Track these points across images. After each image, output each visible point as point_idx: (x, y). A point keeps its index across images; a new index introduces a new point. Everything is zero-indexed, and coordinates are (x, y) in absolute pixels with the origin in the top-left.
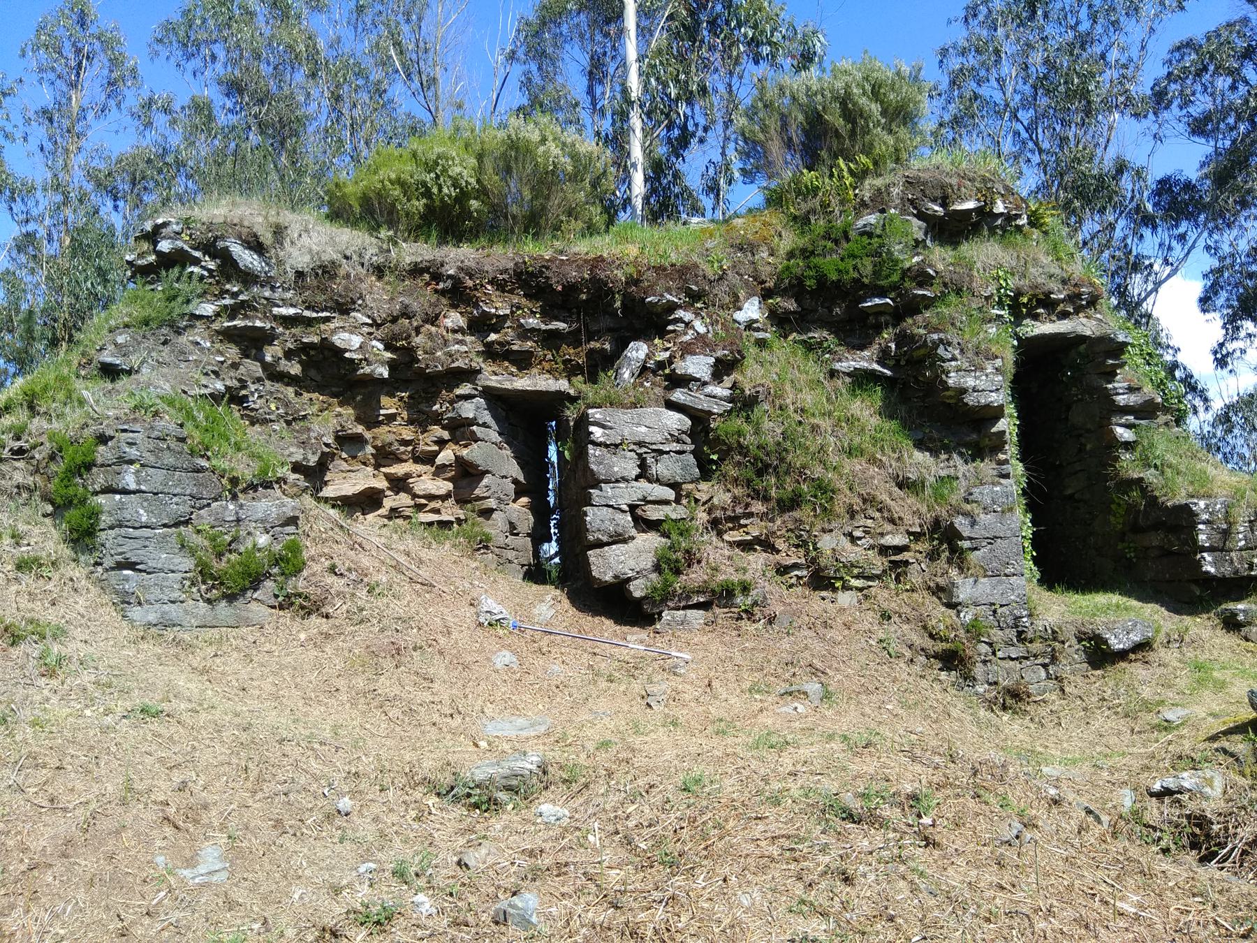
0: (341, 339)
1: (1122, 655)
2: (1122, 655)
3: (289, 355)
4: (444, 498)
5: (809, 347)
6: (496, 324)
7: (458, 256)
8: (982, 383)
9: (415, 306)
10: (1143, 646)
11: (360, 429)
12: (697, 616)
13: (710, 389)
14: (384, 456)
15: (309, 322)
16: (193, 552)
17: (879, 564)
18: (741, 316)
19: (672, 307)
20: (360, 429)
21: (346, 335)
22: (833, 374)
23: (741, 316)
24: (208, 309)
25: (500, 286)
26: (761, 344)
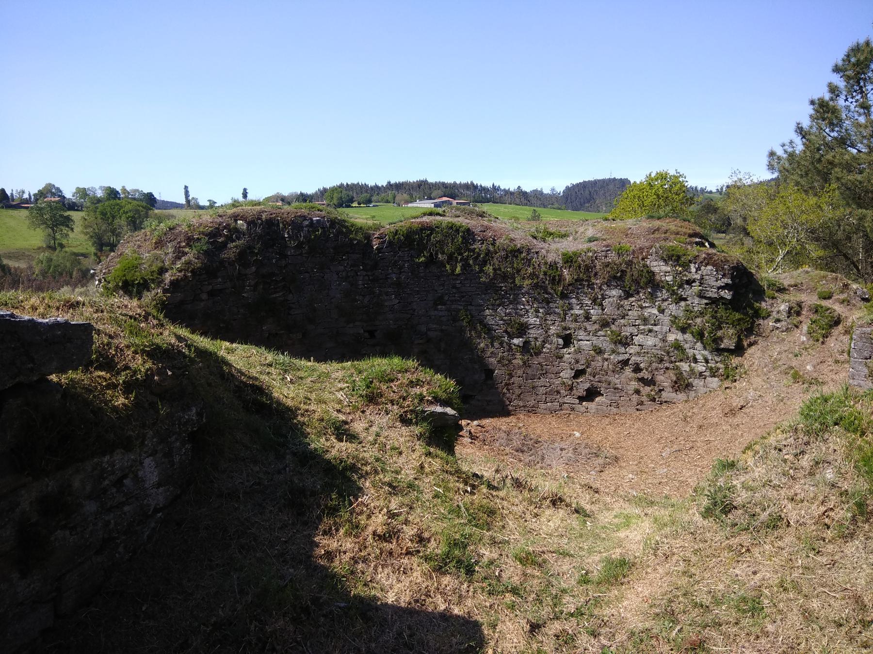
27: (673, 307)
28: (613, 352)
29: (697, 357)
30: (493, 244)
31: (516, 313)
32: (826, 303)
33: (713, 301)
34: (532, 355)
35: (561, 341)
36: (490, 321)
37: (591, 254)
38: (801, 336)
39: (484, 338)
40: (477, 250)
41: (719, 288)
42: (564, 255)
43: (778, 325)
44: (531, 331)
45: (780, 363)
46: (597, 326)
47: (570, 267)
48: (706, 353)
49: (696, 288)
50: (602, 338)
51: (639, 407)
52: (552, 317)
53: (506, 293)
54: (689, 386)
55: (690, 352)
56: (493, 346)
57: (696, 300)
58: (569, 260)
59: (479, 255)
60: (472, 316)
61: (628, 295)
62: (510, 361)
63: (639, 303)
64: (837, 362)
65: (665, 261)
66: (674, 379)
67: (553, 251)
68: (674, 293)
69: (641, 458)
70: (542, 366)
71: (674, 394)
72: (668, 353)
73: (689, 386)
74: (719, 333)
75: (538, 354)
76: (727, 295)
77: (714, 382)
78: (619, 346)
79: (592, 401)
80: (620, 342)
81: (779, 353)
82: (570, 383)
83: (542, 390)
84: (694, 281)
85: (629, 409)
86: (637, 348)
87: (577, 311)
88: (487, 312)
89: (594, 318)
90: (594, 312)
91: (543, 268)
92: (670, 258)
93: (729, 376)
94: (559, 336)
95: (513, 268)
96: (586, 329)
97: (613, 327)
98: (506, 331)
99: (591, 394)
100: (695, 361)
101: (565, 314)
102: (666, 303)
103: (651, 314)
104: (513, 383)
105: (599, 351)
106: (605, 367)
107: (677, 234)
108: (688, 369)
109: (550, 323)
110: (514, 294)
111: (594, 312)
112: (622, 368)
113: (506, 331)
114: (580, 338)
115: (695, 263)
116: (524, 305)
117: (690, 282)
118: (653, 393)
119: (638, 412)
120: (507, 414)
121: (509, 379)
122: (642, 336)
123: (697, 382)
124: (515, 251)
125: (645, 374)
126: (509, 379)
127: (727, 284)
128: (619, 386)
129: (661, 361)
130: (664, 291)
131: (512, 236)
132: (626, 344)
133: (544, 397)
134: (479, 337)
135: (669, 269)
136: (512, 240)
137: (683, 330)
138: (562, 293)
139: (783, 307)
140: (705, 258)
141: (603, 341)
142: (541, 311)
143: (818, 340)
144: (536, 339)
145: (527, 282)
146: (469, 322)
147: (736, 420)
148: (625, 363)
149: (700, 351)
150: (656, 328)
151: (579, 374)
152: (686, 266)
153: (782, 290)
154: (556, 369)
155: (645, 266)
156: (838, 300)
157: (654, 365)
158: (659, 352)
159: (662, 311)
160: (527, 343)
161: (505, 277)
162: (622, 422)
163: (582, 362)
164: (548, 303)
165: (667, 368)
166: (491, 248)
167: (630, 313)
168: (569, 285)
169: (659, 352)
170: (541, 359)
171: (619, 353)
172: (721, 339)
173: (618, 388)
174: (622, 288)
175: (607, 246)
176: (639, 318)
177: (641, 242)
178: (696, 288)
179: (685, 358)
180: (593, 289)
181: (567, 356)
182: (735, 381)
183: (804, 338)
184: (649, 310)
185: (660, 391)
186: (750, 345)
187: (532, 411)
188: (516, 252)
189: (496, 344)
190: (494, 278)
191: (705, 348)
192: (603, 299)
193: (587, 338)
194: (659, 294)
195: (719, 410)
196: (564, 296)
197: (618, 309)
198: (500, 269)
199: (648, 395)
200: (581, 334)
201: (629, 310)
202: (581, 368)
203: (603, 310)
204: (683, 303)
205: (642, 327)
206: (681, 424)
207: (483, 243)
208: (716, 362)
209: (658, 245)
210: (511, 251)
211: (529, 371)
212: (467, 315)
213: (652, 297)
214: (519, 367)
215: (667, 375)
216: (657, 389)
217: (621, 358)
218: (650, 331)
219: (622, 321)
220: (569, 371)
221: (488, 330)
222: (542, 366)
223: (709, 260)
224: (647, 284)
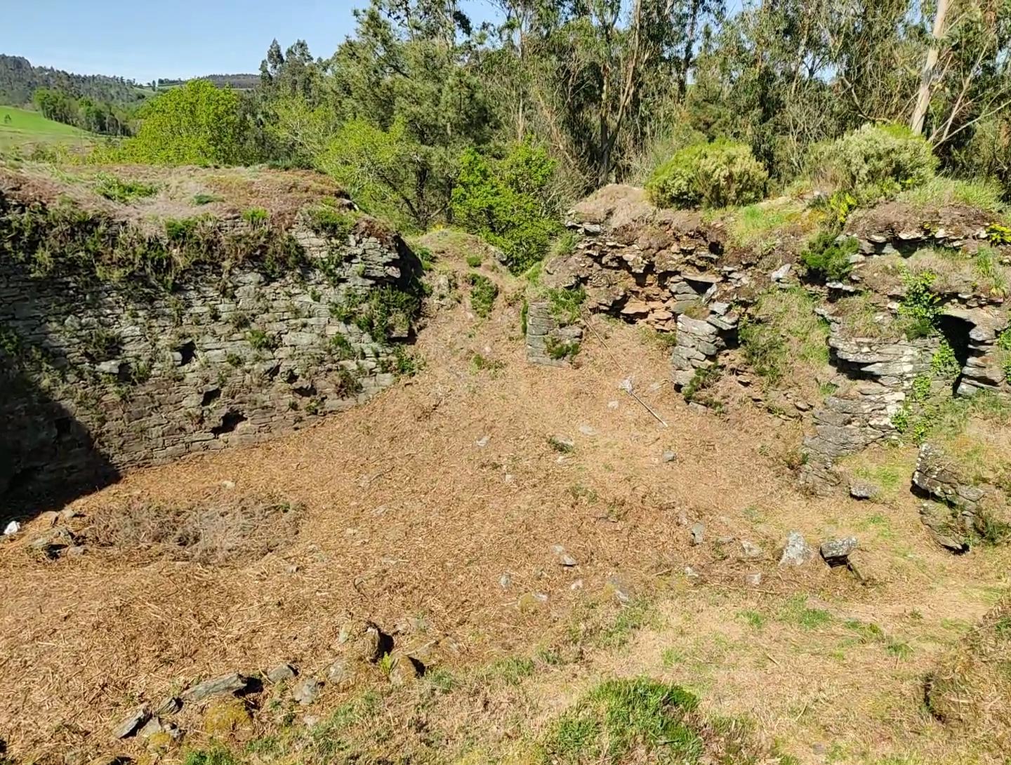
0: (625, 257)
1: (860, 498)
2: (860, 498)
3: (612, 260)
4: (667, 320)
5: (810, 296)
6: (691, 252)
7: (680, 217)
8: (846, 348)
9: (655, 246)
10: (867, 498)
11: (637, 288)
12: (700, 407)
13: (723, 318)
14: (649, 298)
15: (618, 248)
16: (547, 343)
17: (795, 412)
18: (775, 275)
19: (730, 272)
20: (637, 288)
21: (628, 255)
22: (814, 312)
23: (775, 275)
24: (581, 246)
25: (692, 237)
26: (784, 290)
28: (257, 359)
29: (365, 351)
30: (44, 211)
31: (99, 321)
32: (478, 272)
33: (379, 281)
34: (134, 384)
35: (178, 356)
37: (210, 224)
38: (466, 313)
39: (48, 370)
40: (15, 224)
41: (385, 265)
42: (168, 226)
43: (442, 302)
45: (457, 347)
46: (230, 327)
47: (183, 244)
48: (375, 345)
49: (358, 266)
51: (297, 425)
52: (161, 322)
53: (77, 292)
54: (359, 388)
55: (356, 347)
56: (64, 380)
57: (360, 281)
58: (180, 234)
59: (20, 232)
60: (21, 338)
61: (269, 279)
62: (99, 400)
63: (286, 289)
64: (511, 339)
65: (317, 232)
66: (339, 381)
67: (149, 217)
68: (331, 273)
69: (333, 496)
70: (152, 397)
71: (340, 401)
72: (330, 351)
73: (359, 388)
74: (390, 320)
75: (143, 379)
76: (395, 272)
77: (387, 379)
78: (264, 350)
79: (232, 429)
80: (267, 346)
81: (453, 336)
82: (199, 412)
84: (354, 256)
85: (284, 431)
86: (289, 350)
87: (198, 308)
89: (224, 316)
90: (225, 307)
91: (140, 250)
92: (324, 226)
93: (404, 368)
94: (174, 349)
95: (87, 251)
96: (214, 333)
97: (253, 325)
98: (86, 354)
99: (231, 421)
100: (364, 356)
101: (181, 315)
102: (321, 288)
103: (303, 303)
104: (108, 432)
105: (237, 362)
106: (247, 382)
107: (322, 193)
108: (355, 367)
109: (157, 330)
110: (92, 293)
111: (225, 307)
112: (271, 380)
114: (206, 347)
115: (354, 234)
116: (112, 308)
117: (350, 258)
118: (313, 404)
119: (297, 433)
120: (106, 475)
121: (100, 427)
122: (293, 333)
123: (366, 382)
124: (87, 223)
125: (302, 383)
126: (100, 427)
127: (394, 260)
128: (269, 403)
129: (322, 361)
130: (318, 272)
131: (70, 195)
133: (160, 440)
134: (39, 370)
136: (75, 203)
137: (347, 321)
138: (174, 284)
139: (443, 280)
140: (366, 228)
141: (242, 347)
142: (141, 313)
143: (485, 316)
144: (138, 357)
145: (117, 274)
146: (15, 350)
147: (434, 423)
148: (274, 371)
149: (366, 343)
150: (308, 320)
151: (209, 397)
152: (343, 238)
153: (433, 260)
154: (174, 397)
155: (291, 239)
156: (487, 267)
157: (314, 369)
158: (318, 351)
159: (317, 298)
160: (124, 367)
161: (72, 267)
162: (279, 450)
163: (213, 381)
164: (151, 300)
165: (330, 370)
166: (41, 219)
167: (275, 304)
168: (183, 272)
169: (318, 351)
170: (149, 388)
171: (265, 360)
172: (392, 327)
173: (267, 407)
174: (262, 270)
175: (234, 211)
176: (288, 309)
177: (277, 205)
178: (358, 266)
179: (353, 356)
180: (220, 274)
181: (189, 376)
182: (414, 374)
183: (470, 315)
184: (300, 298)
185: (323, 399)
186: (421, 328)
188: (87, 226)
189: (71, 377)
190: (54, 271)
191: (374, 340)
192: (236, 287)
193: (218, 346)
194: (312, 275)
195: (406, 416)
196: (177, 289)
197: (258, 300)
198: (63, 255)
199: (308, 409)
200: (209, 341)
201: (273, 300)
202: (212, 388)
203: (238, 303)
204: (343, 286)
205: (292, 322)
206: (365, 439)
207: (23, 211)
208: (389, 355)
209: (305, 210)
210: (80, 223)
211: (133, 408)
212: (10, 338)
213: (303, 279)
214: (115, 405)
215: (329, 379)
216: (319, 399)
217: (268, 366)
218: (305, 325)
219: (265, 316)
220: (196, 396)
221: (56, 357)
222: (152, 397)
223: (370, 231)
224: (297, 263)
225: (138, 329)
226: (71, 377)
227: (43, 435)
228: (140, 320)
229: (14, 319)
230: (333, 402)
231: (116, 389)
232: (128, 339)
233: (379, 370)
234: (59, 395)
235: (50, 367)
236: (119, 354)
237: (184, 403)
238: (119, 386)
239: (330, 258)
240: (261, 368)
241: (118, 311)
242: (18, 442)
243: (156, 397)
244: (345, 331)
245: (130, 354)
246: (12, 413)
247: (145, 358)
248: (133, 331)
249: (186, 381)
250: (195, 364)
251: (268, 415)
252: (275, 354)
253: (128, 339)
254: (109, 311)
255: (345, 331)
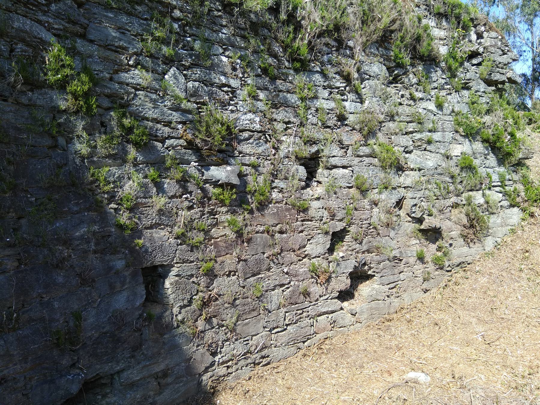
27: (454, 98)
34: (251, 212)
35: (302, 172)
36: (144, 104)
39: (135, 164)
44: (246, 148)
48: (502, 169)
50: (367, 160)
51: (425, 286)
55: (482, 171)
57: (482, 87)
62: (206, 232)
75: (262, 206)
83: (276, 297)
88: (138, 76)
89: (351, 119)
96: (341, 142)
98: (190, 145)
102: (443, 93)
108: (482, 201)
109: (280, 127)
113: (190, 145)
114: (334, 161)
122: (419, 152)
132: (400, 169)
134: (120, 158)
135: (442, 34)
142: (262, 95)
159: (440, 106)
163: (339, 216)
164: (273, 79)
167: (400, 109)
170: (269, 218)
184: (425, 104)
187: (260, 359)
189: (170, 186)
193: (345, 162)
202: (340, 226)
204: (465, 93)
205: (418, 136)
218: (429, 142)
219: (391, 124)
225: (258, 119)
226: (170, 186)
227: (120, 301)
228: (260, 105)
229: (83, 36)
230: (460, 251)
231: (229, 217)
232: (246, 135)
233: (505, 203)
234: (151, 215)
235: (140, 158)
236: (233, 157)
237: (308, 248)
238: (234, 212)
239: (452, 55)
240: (388, 199)
241: (234, 83)
242: (78, 317)
243: (277, 236)
244: (470, 152)
245: (247, 160)
246: (67, 242)
247: (266, 167)
248: (252, 121)
249: (312, 212)
250: (318, 190)
251: (396, 271)
252: (402, 179)
253: (246, 135)
254: (223, 79)
255: (470, 152)
